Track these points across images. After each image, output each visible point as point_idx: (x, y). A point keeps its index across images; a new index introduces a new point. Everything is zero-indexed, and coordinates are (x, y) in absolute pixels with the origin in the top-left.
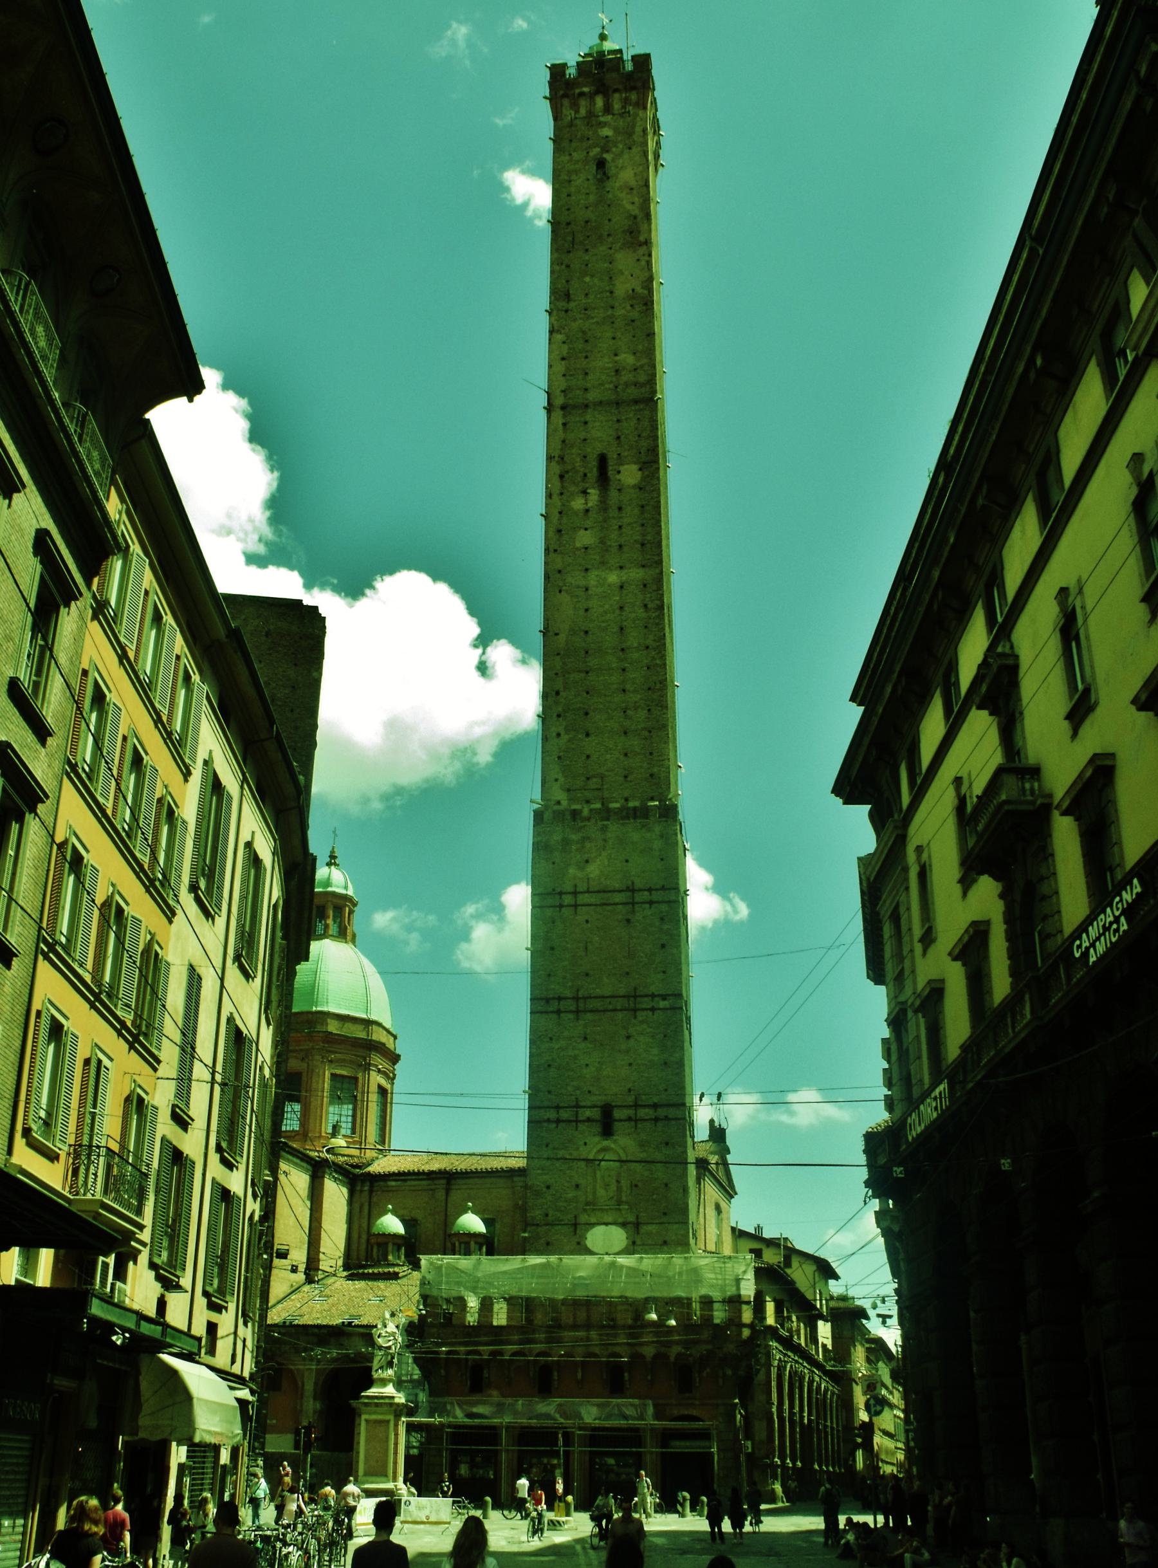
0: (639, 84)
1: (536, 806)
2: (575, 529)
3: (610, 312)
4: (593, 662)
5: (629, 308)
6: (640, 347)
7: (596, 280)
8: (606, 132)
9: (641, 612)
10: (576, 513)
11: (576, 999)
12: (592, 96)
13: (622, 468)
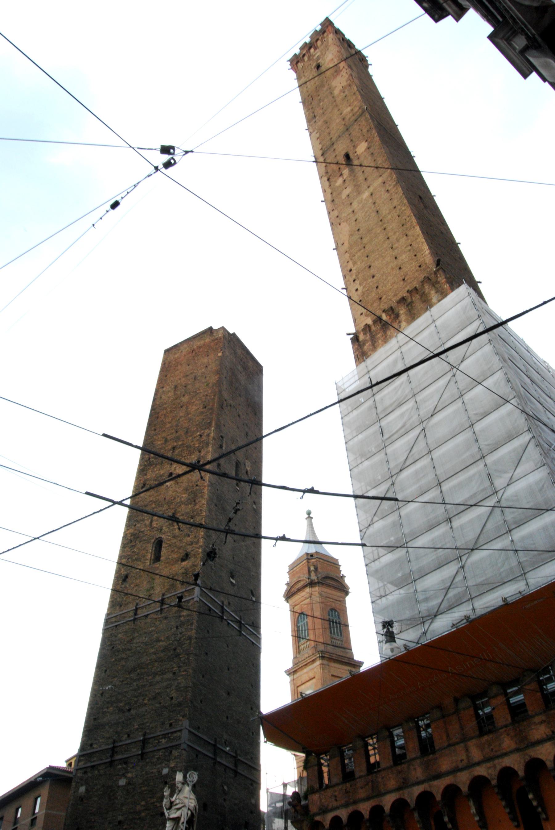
1: (352, 336)
2: (340, 193)
3: (334, 104)
4: (365, 240)
5: (342, 94)
6: (352, 101)
7: (326, 100)
9: (387, 195)
10: (339, 187)
13: (357, 150)
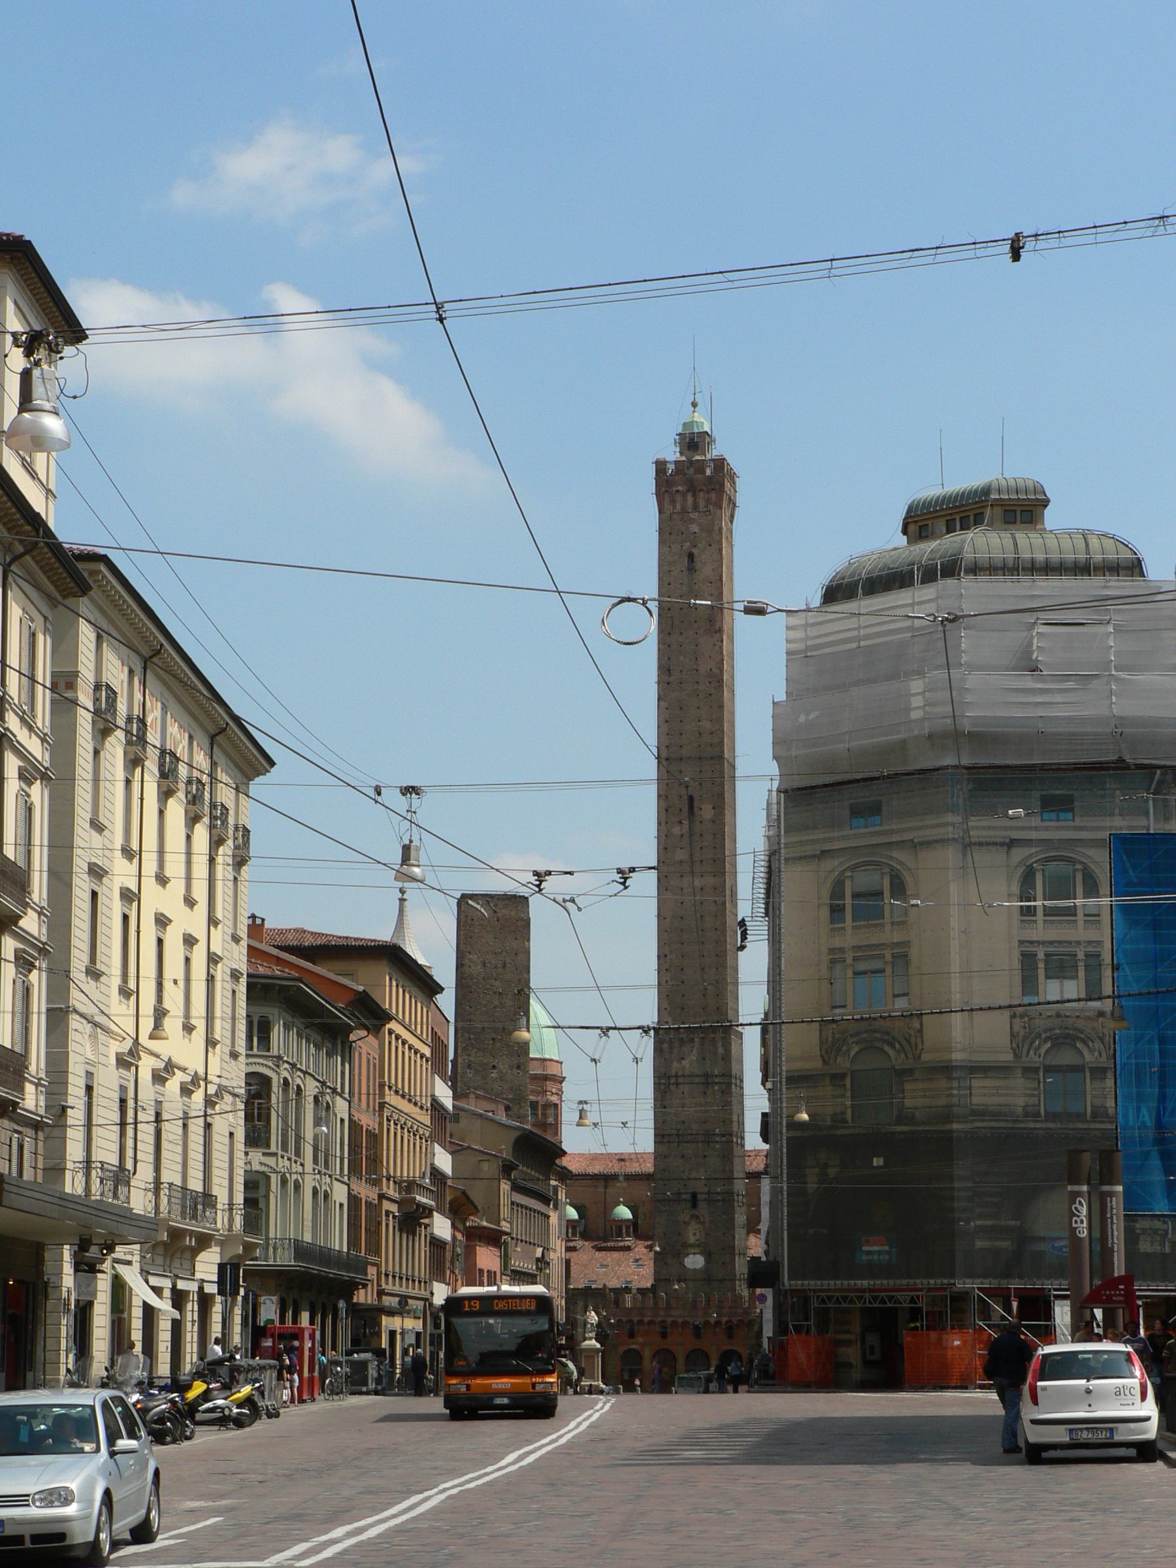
0: (717, 487)
8: (694, 528)
11: (678, 1135)
12: (684, 495)
